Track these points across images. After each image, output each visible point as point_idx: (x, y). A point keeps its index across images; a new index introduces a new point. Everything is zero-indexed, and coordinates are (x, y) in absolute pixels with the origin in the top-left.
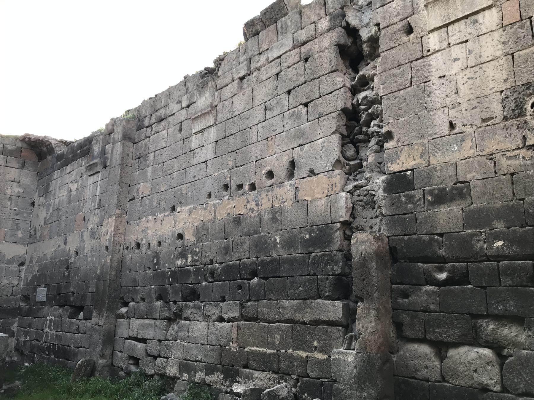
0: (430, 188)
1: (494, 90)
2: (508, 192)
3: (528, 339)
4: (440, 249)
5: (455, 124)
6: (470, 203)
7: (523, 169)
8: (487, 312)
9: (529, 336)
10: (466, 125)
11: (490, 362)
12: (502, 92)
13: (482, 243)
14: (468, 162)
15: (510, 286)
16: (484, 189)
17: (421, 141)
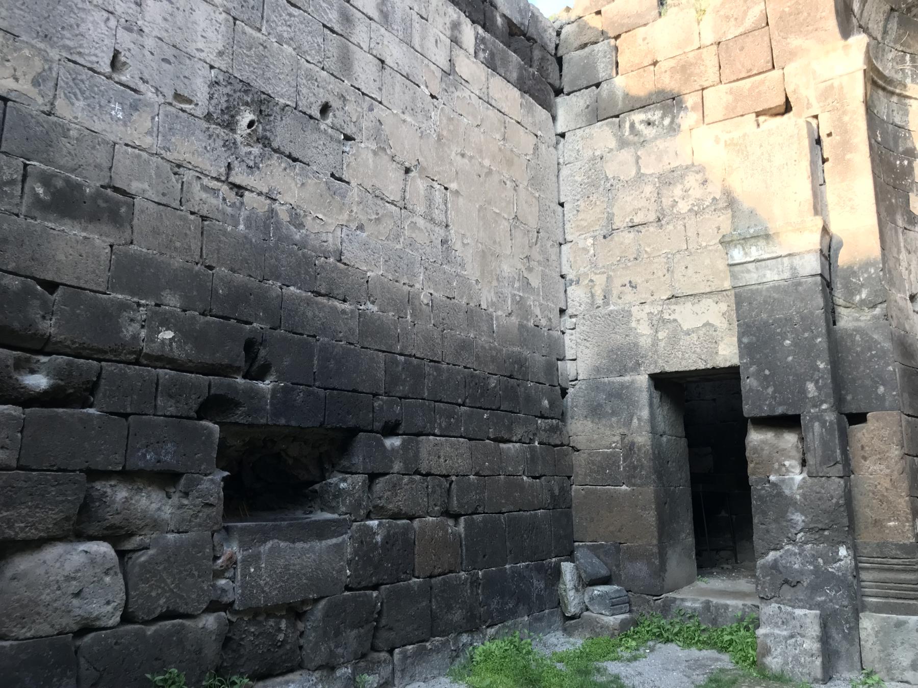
0: (43, 166)
1: (203, 55)
2: (195, 245)
3: (179, 512)
4: (44, 317)
5: (125, 64)
6: (129, 241)
7: (220, 217)
8: (124, 467)
9: (181, 506)
10: (147, 83)
11: (111, 569)
12: (212, 67)
13: (137, 326)
14: (139, 156)
15: (172, 416)
16: (159, 224)
17: (42, 45)
